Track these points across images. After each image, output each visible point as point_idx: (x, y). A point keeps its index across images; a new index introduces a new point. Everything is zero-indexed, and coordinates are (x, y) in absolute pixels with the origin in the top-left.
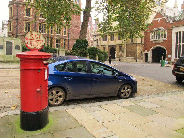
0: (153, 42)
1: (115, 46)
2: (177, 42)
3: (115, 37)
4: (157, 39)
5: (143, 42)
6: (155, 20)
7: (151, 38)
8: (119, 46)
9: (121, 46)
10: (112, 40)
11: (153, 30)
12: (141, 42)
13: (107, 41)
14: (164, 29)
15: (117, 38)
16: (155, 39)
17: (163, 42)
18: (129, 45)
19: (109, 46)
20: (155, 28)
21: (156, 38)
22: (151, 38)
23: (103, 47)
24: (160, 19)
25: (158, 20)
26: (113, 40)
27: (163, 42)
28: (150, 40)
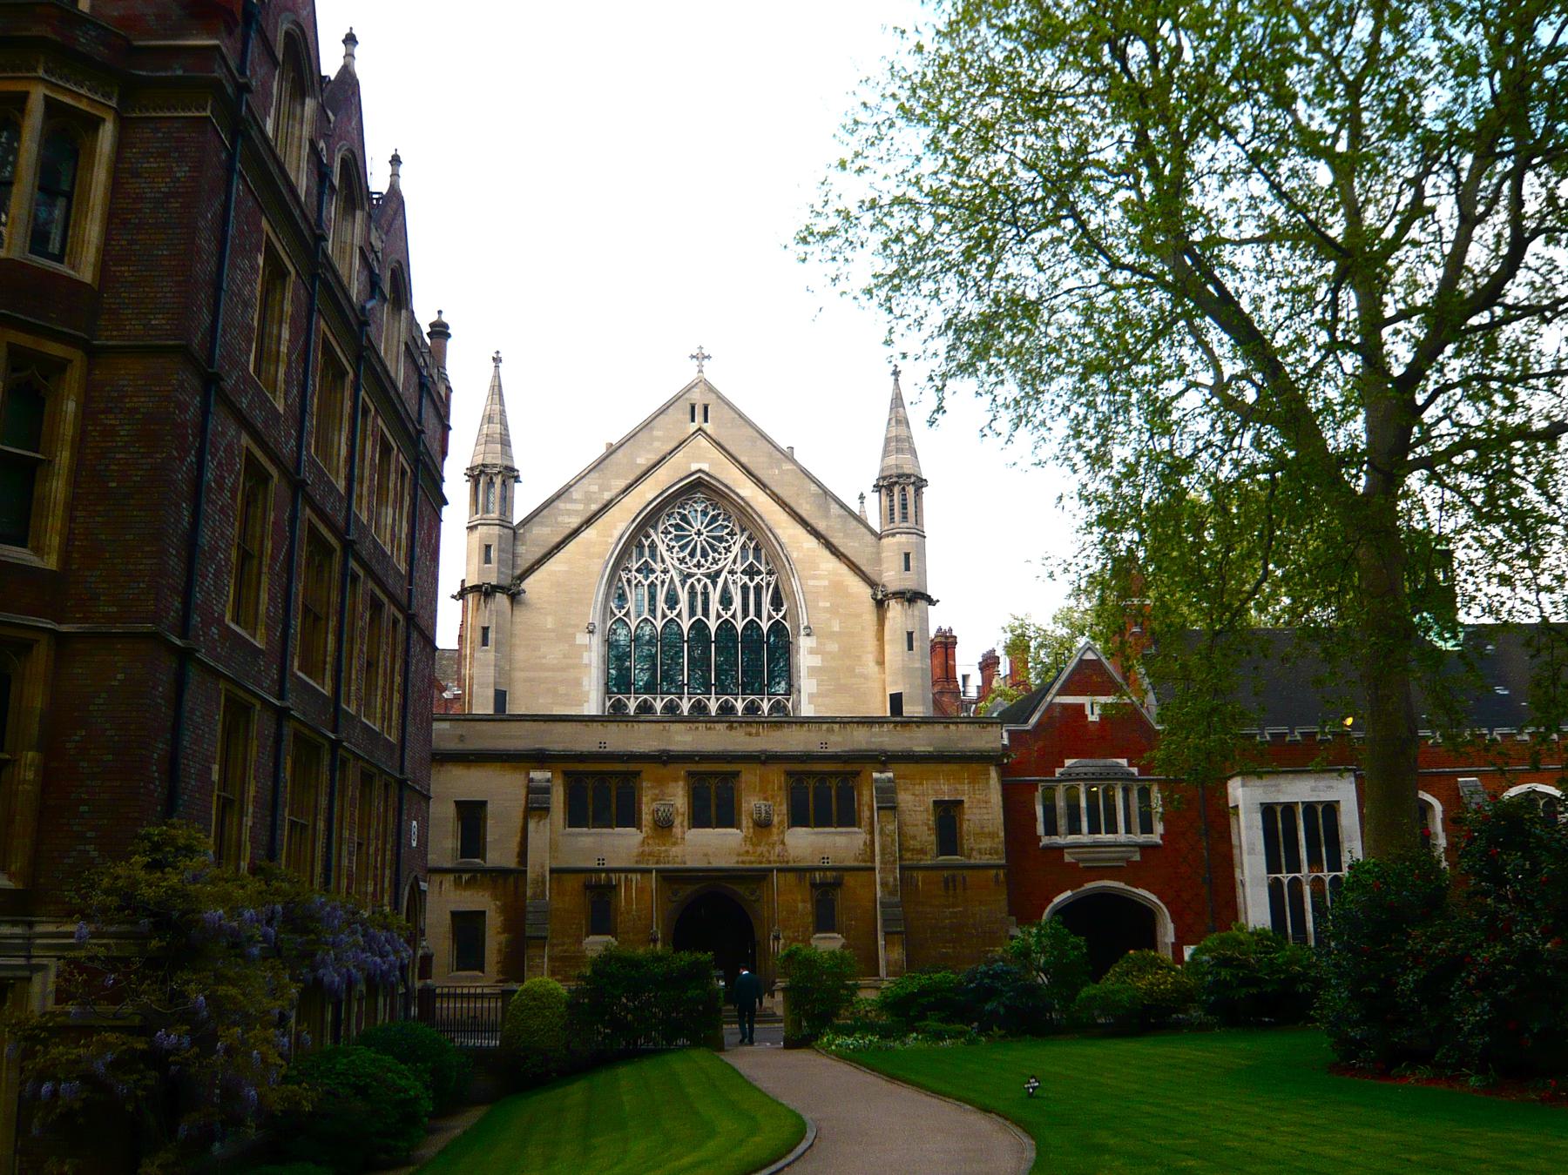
0: (1068, 858)
1: (757, 877)
2: (1273, 866)
3: (751, 803)
4: (1104, 837)
6: (1065, 706)
7: (1040, 829)
8: (813, 885)
9: (838, 884)
10: (699, 819)
11: (1058, 771)
14: (1135, 770)
15: (780, 812)
16: (1085, 838)
17: (1137, 857)
20: (1068, 762)
21: (1094, 829)
22: (1040, 829)
23: (572, 883)
24: (1103, 699)
25: (1088, 711)
27: (1137, 857)
28: (1039, 839)
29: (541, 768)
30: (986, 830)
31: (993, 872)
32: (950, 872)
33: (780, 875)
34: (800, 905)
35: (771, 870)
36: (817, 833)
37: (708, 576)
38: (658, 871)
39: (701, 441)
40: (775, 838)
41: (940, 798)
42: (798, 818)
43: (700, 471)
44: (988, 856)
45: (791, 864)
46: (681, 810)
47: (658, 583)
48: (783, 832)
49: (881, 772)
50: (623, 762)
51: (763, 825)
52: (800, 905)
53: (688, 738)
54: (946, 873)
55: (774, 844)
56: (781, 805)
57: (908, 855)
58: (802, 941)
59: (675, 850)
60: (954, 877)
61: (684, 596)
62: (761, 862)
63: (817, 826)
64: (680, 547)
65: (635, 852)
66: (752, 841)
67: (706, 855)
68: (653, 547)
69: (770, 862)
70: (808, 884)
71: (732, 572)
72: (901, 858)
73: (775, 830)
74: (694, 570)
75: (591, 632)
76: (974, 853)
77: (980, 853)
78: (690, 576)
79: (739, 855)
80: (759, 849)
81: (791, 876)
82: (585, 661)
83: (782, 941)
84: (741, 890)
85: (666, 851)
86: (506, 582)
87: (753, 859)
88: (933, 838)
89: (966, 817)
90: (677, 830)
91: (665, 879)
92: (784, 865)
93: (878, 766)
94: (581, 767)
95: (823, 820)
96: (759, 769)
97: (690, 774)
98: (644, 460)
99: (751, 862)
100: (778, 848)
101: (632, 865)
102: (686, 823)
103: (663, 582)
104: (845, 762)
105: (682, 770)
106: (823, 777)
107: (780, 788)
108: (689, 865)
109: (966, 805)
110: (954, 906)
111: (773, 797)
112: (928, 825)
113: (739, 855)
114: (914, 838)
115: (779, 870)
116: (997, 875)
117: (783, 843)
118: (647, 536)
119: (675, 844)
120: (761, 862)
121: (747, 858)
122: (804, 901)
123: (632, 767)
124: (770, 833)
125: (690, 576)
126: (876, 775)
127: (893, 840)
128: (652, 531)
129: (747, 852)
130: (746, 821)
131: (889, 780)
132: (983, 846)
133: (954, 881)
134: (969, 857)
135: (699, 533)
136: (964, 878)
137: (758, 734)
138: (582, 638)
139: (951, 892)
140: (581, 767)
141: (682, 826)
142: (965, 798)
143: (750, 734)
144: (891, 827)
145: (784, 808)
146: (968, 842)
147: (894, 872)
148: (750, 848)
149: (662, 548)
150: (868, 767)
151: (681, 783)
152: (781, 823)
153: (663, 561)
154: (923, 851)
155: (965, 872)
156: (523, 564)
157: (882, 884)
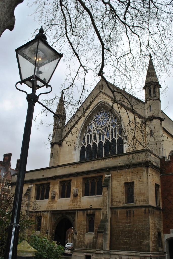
3: (73, 188)
5: (161, 203)
8: (87, 215)
9: (94, 215)
12: (156, 204)
13: (47, 198)
15: (80, 191)
18: (118, 211)
19: (54, 213)
26: (69, 196)
29: (31, 184)
30: (142, 192)
31: (143, 209)
32: (129, 209)
33: (79, 212)
34: (83, 222)
35: (75, 210)
36: (89, 198)
37: (103, 129)
38: (51, 211)
39: (101, 95)
40: (78, 200)
41: (126, 181)
42: (86, 193)
43: (100, 102)
44: (142, 203)
45: (82, 208)
46: (57, 193)
47: (92, 134)
48: (80, 198)
49: (108, 175)
50: (47, 180)
51: (76, 195)
52: (83, 222)
53: (60, 171)
54: (127, 210)
55: (78, 202)
56: (80, 189)
57: (115, 204)
58: (82, 235)
59: (55, 205)
60: (130, 211)
61: (98, 136)
62: (74, 208)
63: (91, 195)
64: (99, 125)
65: (46, 206)
66: (73, 201)
67: (61, 206)
68: (91, 125)
69: (76, 208)
70: (85, 215)
71: (109, 126)
72: (112, 205)
73: (78, 197)
74: (101, 128)
75: (75, 150)
76: (137, 202)
77: (139, 201)
78: (100, 130)
79: (69, 206)
80: (74, 204)
81: (81, 212)
82: (74, 158)
83: (77, 235)
84: (70, 217)
85: (53, 205)
86: (57, 141)
87: (72, 207)
88: (124, 197)
89: (135, 188)
90: (56, 199)
91: (52, 213)
92: (80, 208)
93: (107, 173)
94: (39, 183)
95: (93, 194)
96: (75, 178)
97: (61, 182)
98: (88, 104)
99: (72, 208)
100: (79, 203)
101: (46, 210)
102: (58, 197)
103: (93, 134)
104: (98, 173)
105: (58, 181)
106: (93, 178)
107: (81, 183)
108: (58, 209)
109: (135, 183)
110: (130, 222)
111: (79, 186)
112: (122, 192)
113: (69, 206)
114: (117, 197)
115: (78, 210)
116: (145, 210)
117: (80, 201)
118: (90, 123)
119: (55, 203)
120: (74, 208)
121: (71, 207)
122: (84, 221)
123: (49, 181)
124: (77, 198)
125: (100, 130)
126: (106, 176)
127: (106, 198)
128: (91, 121)
129: (71, 205)
130: (72, 195)
131: (109, 177)
132: (141, 199)
133: (130, 213)
134: (136, 203)
135: (102, 118)
136: (133, 212)
137: (76, 167)
138: (74, 152)
139: (129, 217)
140: (39, 183)
141: (57, 198)
142: (134, 181)
143: (74, 168)
144: (106, 193)
145: (81, 190)
146: (136, 197)
147: (106, 210)
148: (72, 203)
149: (93, 125)
150: (105, 173)
151: (58, 185)
152: (80, 194)
153: (93, 128)
154: (120, 202)
155: (134, 209)
156: (63, 137)
157: (102, 214)
